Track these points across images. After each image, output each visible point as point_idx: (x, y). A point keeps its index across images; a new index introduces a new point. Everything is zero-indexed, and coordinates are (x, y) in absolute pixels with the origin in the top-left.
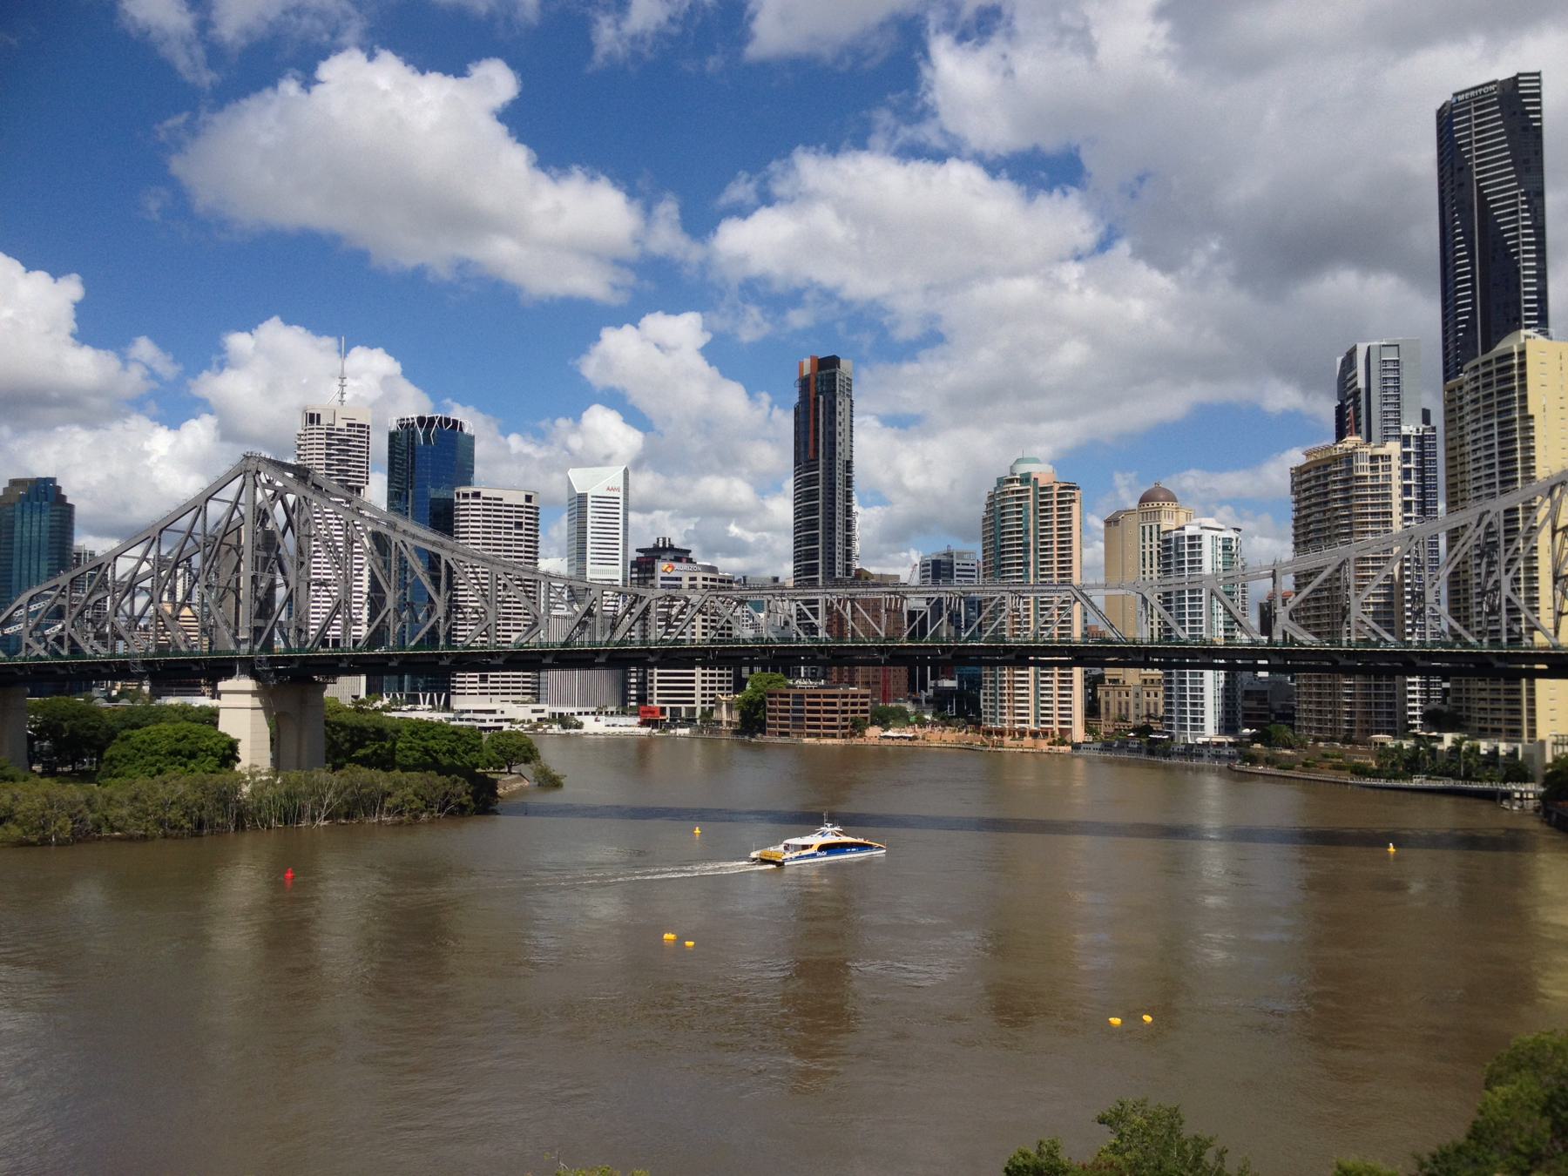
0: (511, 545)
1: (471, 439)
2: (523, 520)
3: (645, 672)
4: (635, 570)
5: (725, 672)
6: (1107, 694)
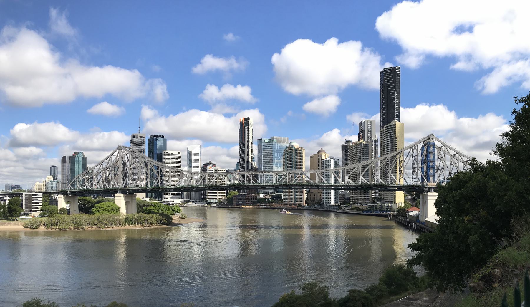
3: (206, 192)
4: (203, 169)
5: (224, 191)
6: (310, 195)
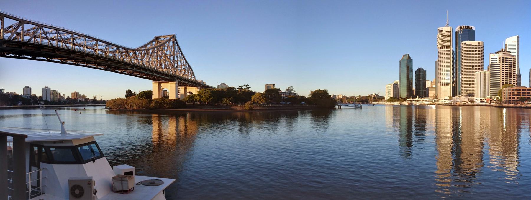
1: (474, 31)
2: (477, 49)
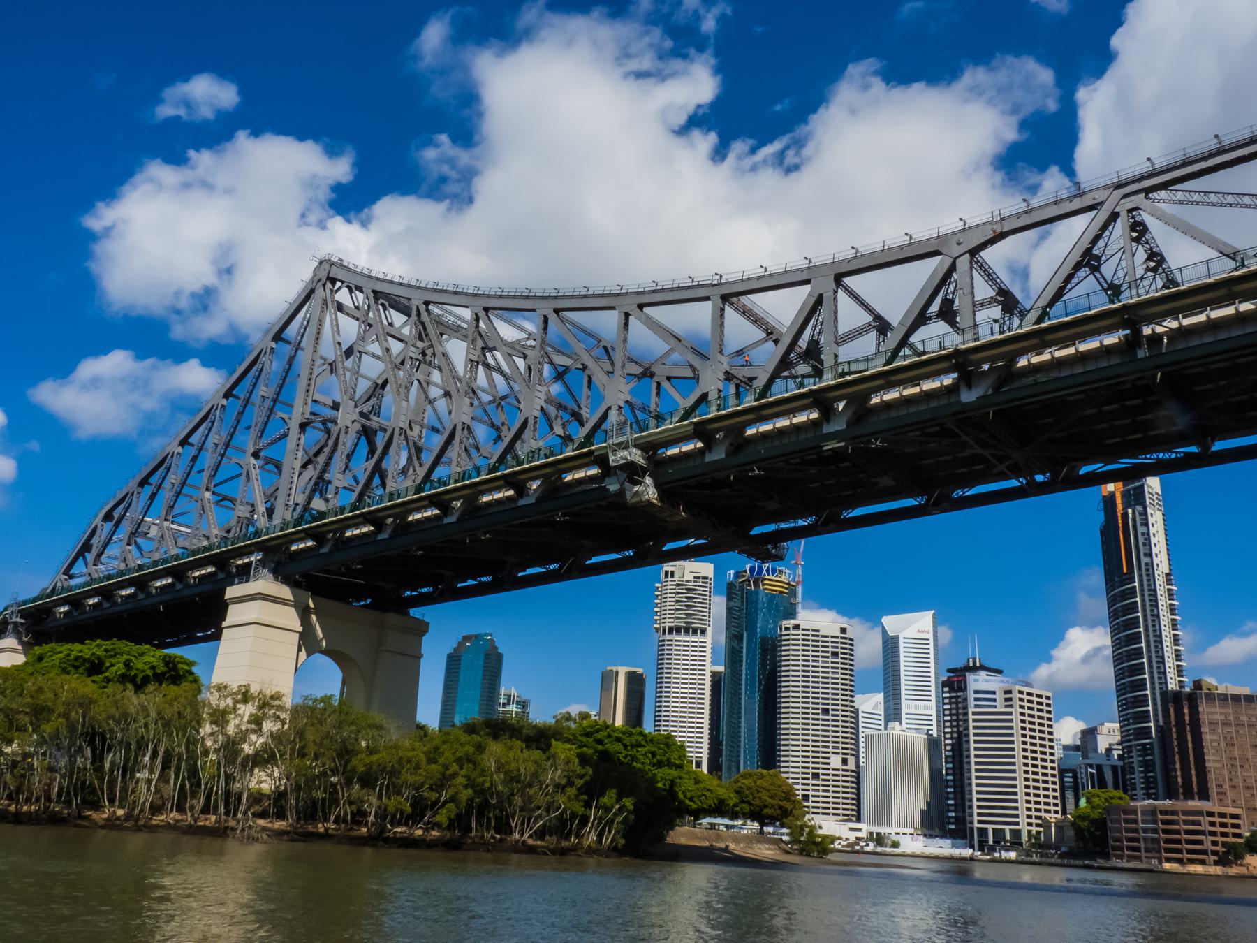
0: (828, 673)
4: (946, 689)
